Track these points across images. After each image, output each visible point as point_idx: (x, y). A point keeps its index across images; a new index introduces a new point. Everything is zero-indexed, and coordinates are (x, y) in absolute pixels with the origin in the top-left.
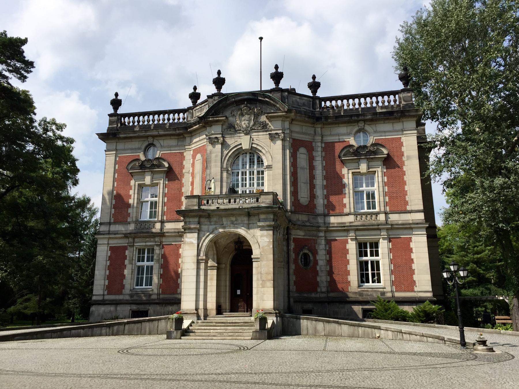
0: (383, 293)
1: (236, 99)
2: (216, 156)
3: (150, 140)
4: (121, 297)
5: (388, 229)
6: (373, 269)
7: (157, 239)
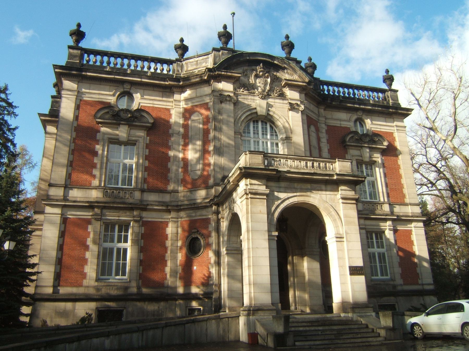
0: (394, 286)
3: (127, 87)
4: (81, 290)
5: (393, 220)
6: (380, 262)
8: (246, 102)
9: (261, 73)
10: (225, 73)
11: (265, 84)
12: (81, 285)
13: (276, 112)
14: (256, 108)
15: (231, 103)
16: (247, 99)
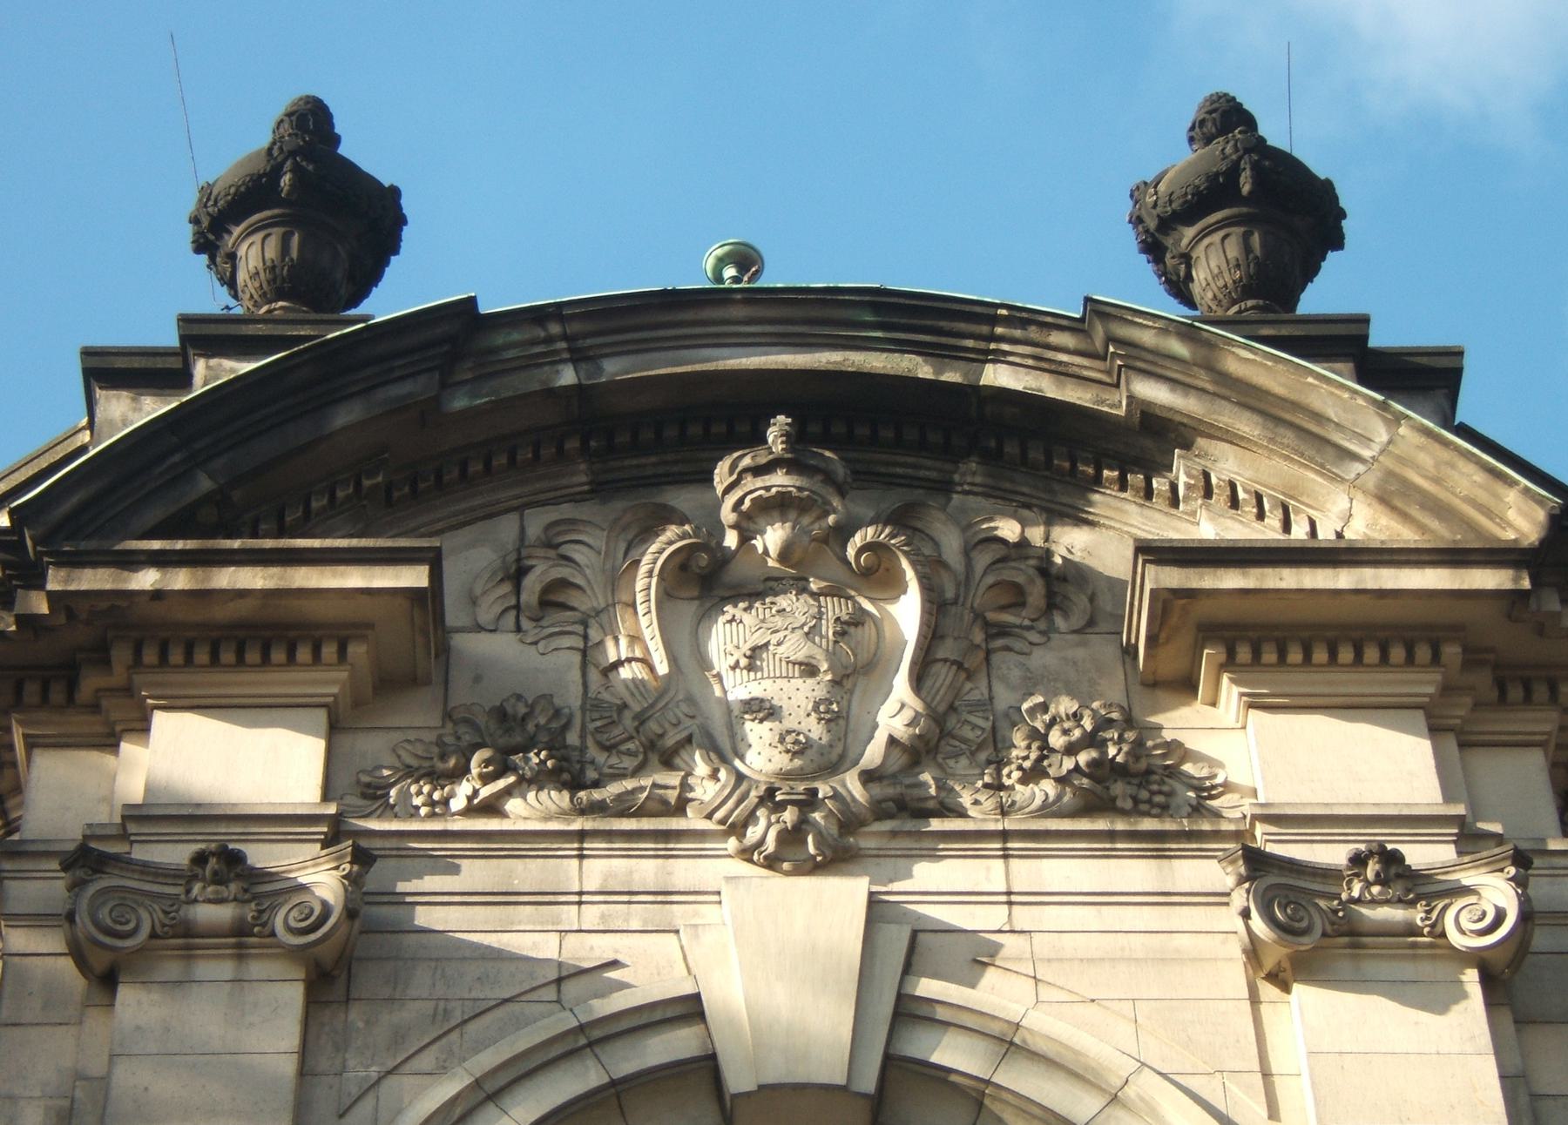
1: (614, 368)
8: (534, 940)
9: (773, 537)
10: (181, 580)
11: (852, 674)
13: (1047, 1023)
14: (690, 1009)
15: (257, 969)
16: (547, 898)
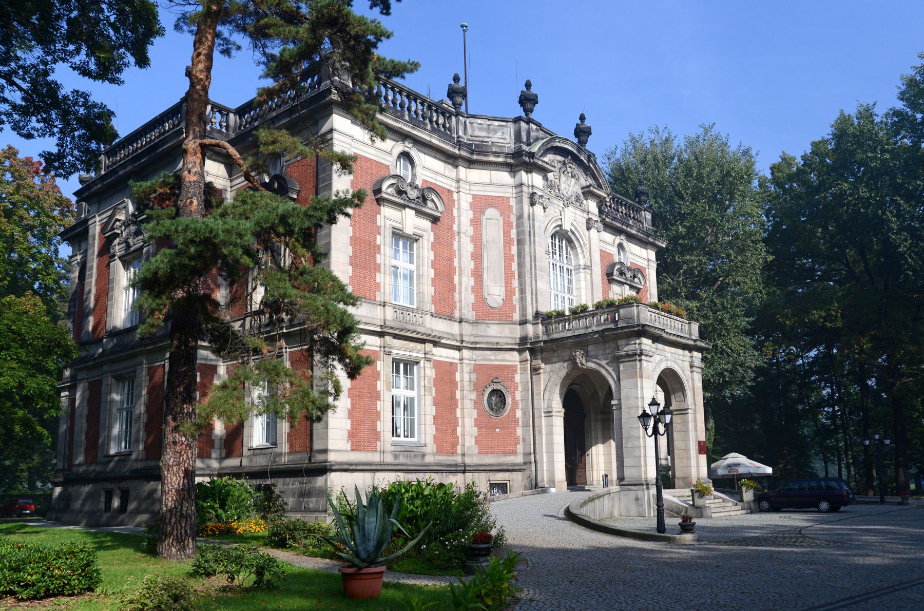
2: (540, 227)
3: (408, 146)
4: (374, 457)
7: (429, 346)
12: (374, 450)
